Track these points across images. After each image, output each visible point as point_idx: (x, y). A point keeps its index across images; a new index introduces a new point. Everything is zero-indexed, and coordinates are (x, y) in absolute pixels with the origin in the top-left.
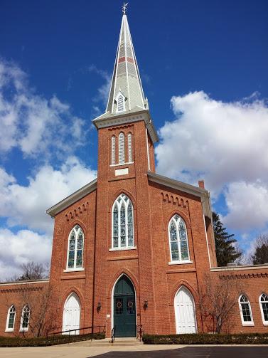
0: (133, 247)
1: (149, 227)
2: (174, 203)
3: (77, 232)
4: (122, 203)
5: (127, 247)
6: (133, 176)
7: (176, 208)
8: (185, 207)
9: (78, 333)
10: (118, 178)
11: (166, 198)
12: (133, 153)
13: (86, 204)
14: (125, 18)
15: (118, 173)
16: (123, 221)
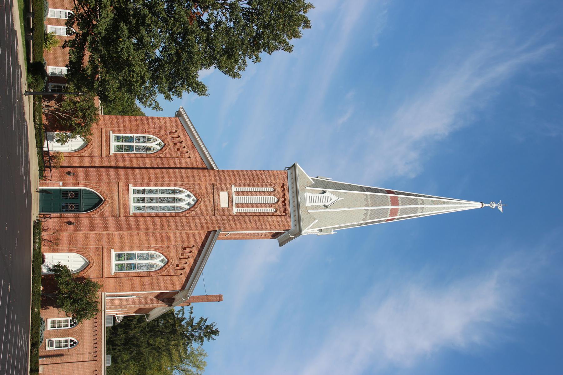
0: (132, 211)
1: (153, 229)
2: (180, 260)
5: (132, 205)
6: (216, 212)
7: (174, 262)
8: (175, 271)
9: (45, 149)
10: (216, 195)
11: (188, 250)
12: (248, 214)
13: (188, 155)
14: (477, 205)
15: (223, 195)
16: (162, 200)
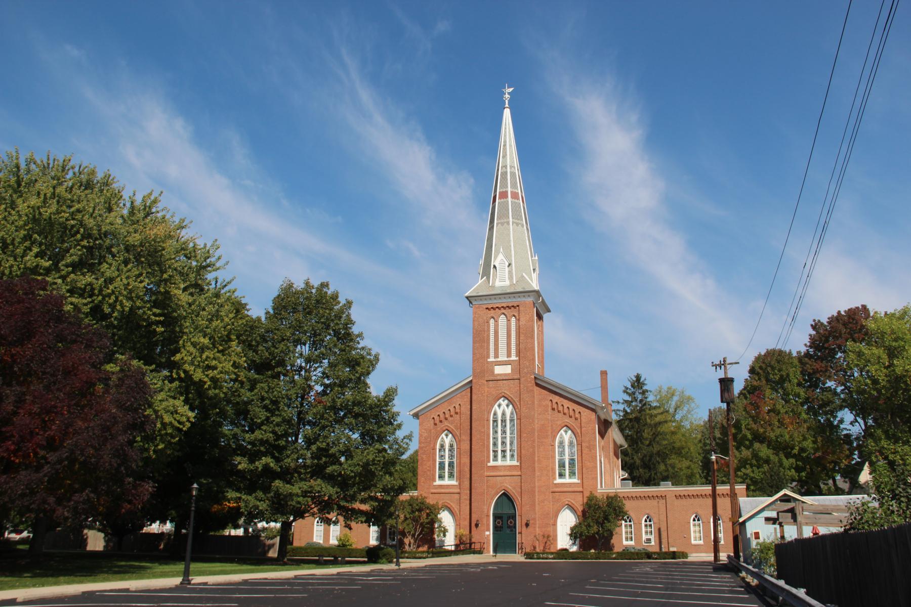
0: (515, 463)
1: (534, 441)
2: (565, 414)
3: (448, 440)
4: (503, 408)
5: (508, 462)
6: (516, 377)
7: (567, 420)
8: (576, 419)
9: (453, 548)
10: (499, 378)
11: (555, 406)
12: (518, 345)
13: (457, 407)
14: (507, 113)
15: (498, 370)
16: (504, 432)
